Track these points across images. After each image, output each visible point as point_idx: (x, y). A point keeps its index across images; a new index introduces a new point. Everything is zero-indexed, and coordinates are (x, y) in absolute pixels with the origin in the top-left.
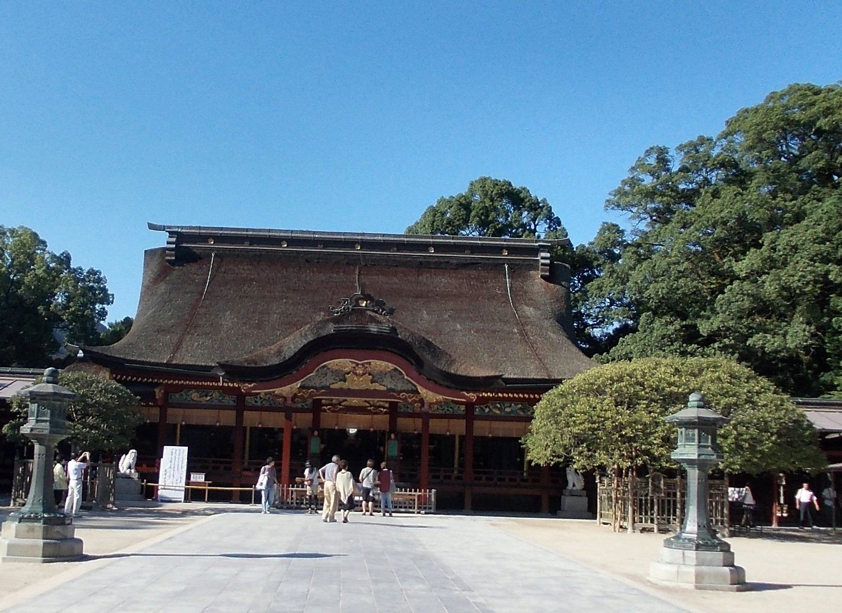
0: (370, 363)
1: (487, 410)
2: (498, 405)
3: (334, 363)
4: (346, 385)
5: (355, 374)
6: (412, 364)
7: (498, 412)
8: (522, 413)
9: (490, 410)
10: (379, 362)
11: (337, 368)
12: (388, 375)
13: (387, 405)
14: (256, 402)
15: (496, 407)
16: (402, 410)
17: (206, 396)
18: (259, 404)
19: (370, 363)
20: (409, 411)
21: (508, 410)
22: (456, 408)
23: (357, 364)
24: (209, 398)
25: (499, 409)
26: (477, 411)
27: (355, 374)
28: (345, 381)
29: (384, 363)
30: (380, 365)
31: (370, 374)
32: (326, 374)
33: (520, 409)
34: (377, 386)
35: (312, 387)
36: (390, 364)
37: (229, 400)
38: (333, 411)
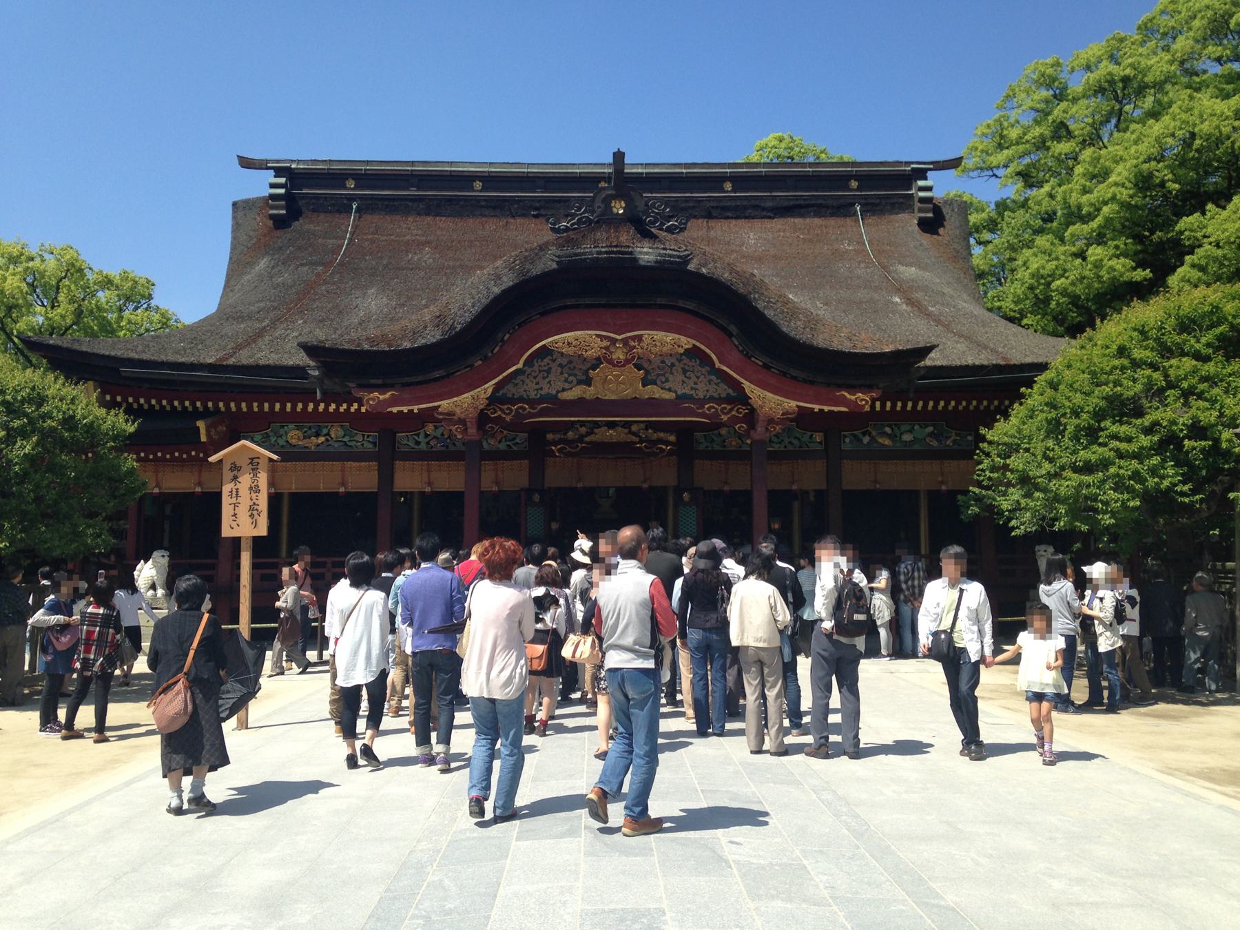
0: (640, 338)
1: (866, 440)
2: (888, 430)
3: (563, 340)
4: (590, 392)
5: (610, 362)
6: (730, 335)
7: (887, 442)
8: (935, 443)
9: (873, 439)
10: (659, 335)
11: (570, 351)
12: (679, 366)
13: (672, 438)
14: (418, 443)
15: (884, 434)
16: (702, 447)
17: (317, 435)
18: (423, 446)
19: (640, 338)
20: (717, 448)
21: (907, 437)
22: (806, 438)
23: (614, 341)
24: (322, 439)
25: (889, 436)
26: (847, 444)
27: (610, 362)
28: (588, 382)
29: (670, 337)
30: (663, 340)
31: (639, 367)
32: (549, 371)
33: (931, 434)
34: (656, 392)
35: (521, 400)
36: (683, 339)
37: (363, 441)
38: (568, 455)
